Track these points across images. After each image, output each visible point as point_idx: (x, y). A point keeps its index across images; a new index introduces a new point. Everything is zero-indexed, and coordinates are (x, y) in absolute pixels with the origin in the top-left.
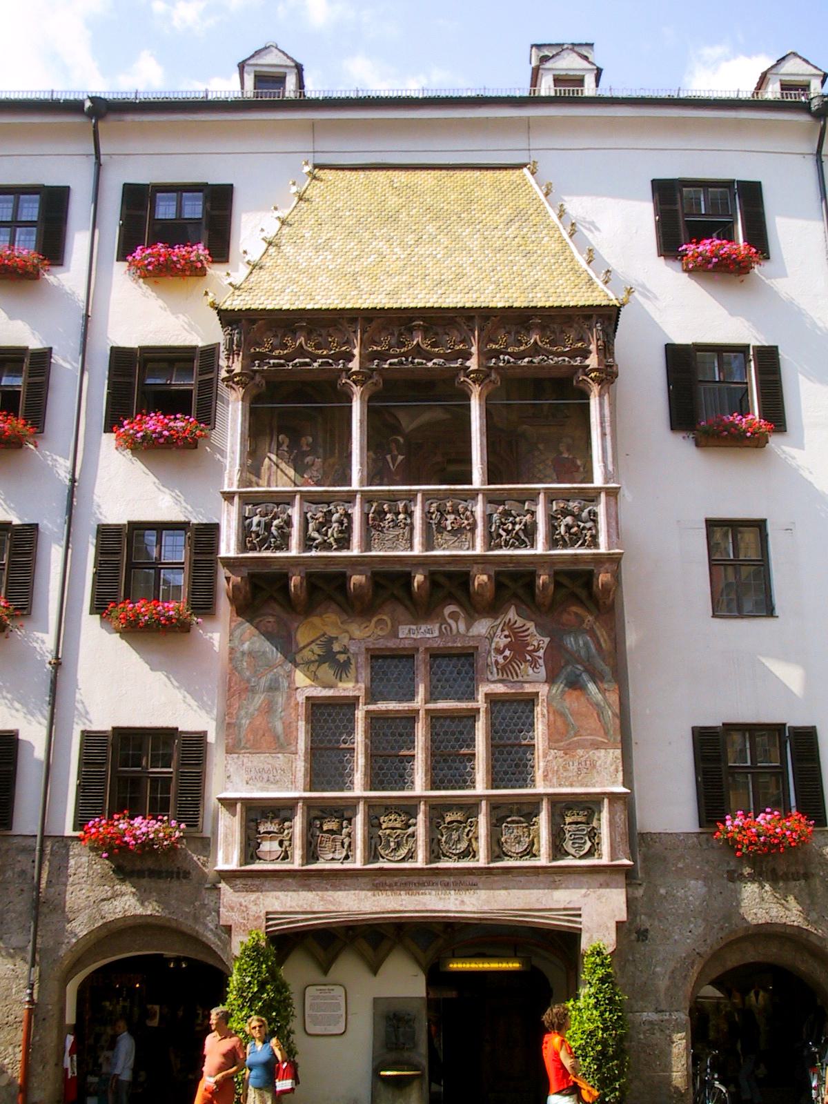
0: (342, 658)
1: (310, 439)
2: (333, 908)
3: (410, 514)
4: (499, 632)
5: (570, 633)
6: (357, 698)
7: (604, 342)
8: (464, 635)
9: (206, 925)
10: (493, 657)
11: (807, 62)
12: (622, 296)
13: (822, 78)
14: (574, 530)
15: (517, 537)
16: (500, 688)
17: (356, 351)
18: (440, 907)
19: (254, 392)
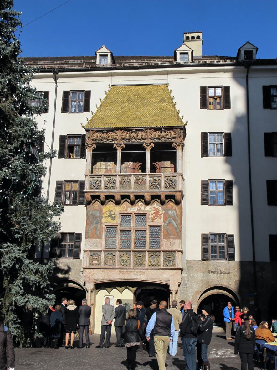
0: (114, 216)
1: (109, 159)
2: (110, 277)
3: (130, 180)
4: (152, 210)
5: (170, 210)
6: (117, 225)
7: (180, 135)
8: (144, 210)
9: (80, 280)
10: (151, 216)
11: (252, 44)
12: (186, 123)
13: (256, 49)
14: (171, 184)
15: (156, 186)
16: (152, 224)
17: (118, 138)
18: (135, 277)
19: (93, 148)
